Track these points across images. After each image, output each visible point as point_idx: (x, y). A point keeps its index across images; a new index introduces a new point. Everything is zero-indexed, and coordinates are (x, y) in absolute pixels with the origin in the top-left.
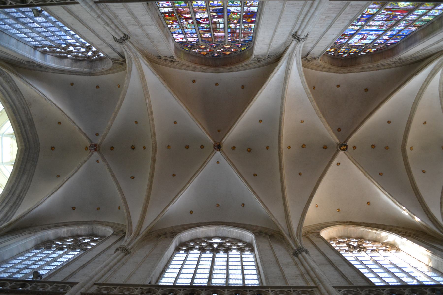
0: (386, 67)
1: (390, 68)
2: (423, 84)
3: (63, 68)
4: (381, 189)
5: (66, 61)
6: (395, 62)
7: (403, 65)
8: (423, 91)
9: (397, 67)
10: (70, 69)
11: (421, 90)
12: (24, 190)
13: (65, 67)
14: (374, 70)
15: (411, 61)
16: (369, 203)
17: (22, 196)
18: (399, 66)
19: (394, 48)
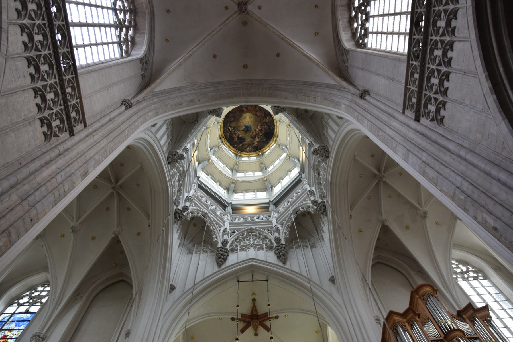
3: (147, 41)
5: (137, 39)
10: (148, 34)
13: (145, 39)
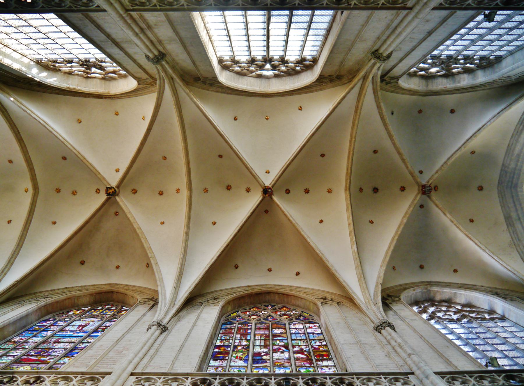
0: (57, 291)
1: (51, 290)
2: (9, 269)
4: (62, 139)
5: (463, 301)
6: (45, 297)
7: (34, 294)
8: (9, 261)
9: (43, 292)
10: (457, 290)
11: (11, 262)
12: (518, 134)
13: (463, 293)
14: (72, 287)
15: (24, 299)
16: (80, 122)
17: (520, 126)
18: (40, 292)
19: (45, 316)
